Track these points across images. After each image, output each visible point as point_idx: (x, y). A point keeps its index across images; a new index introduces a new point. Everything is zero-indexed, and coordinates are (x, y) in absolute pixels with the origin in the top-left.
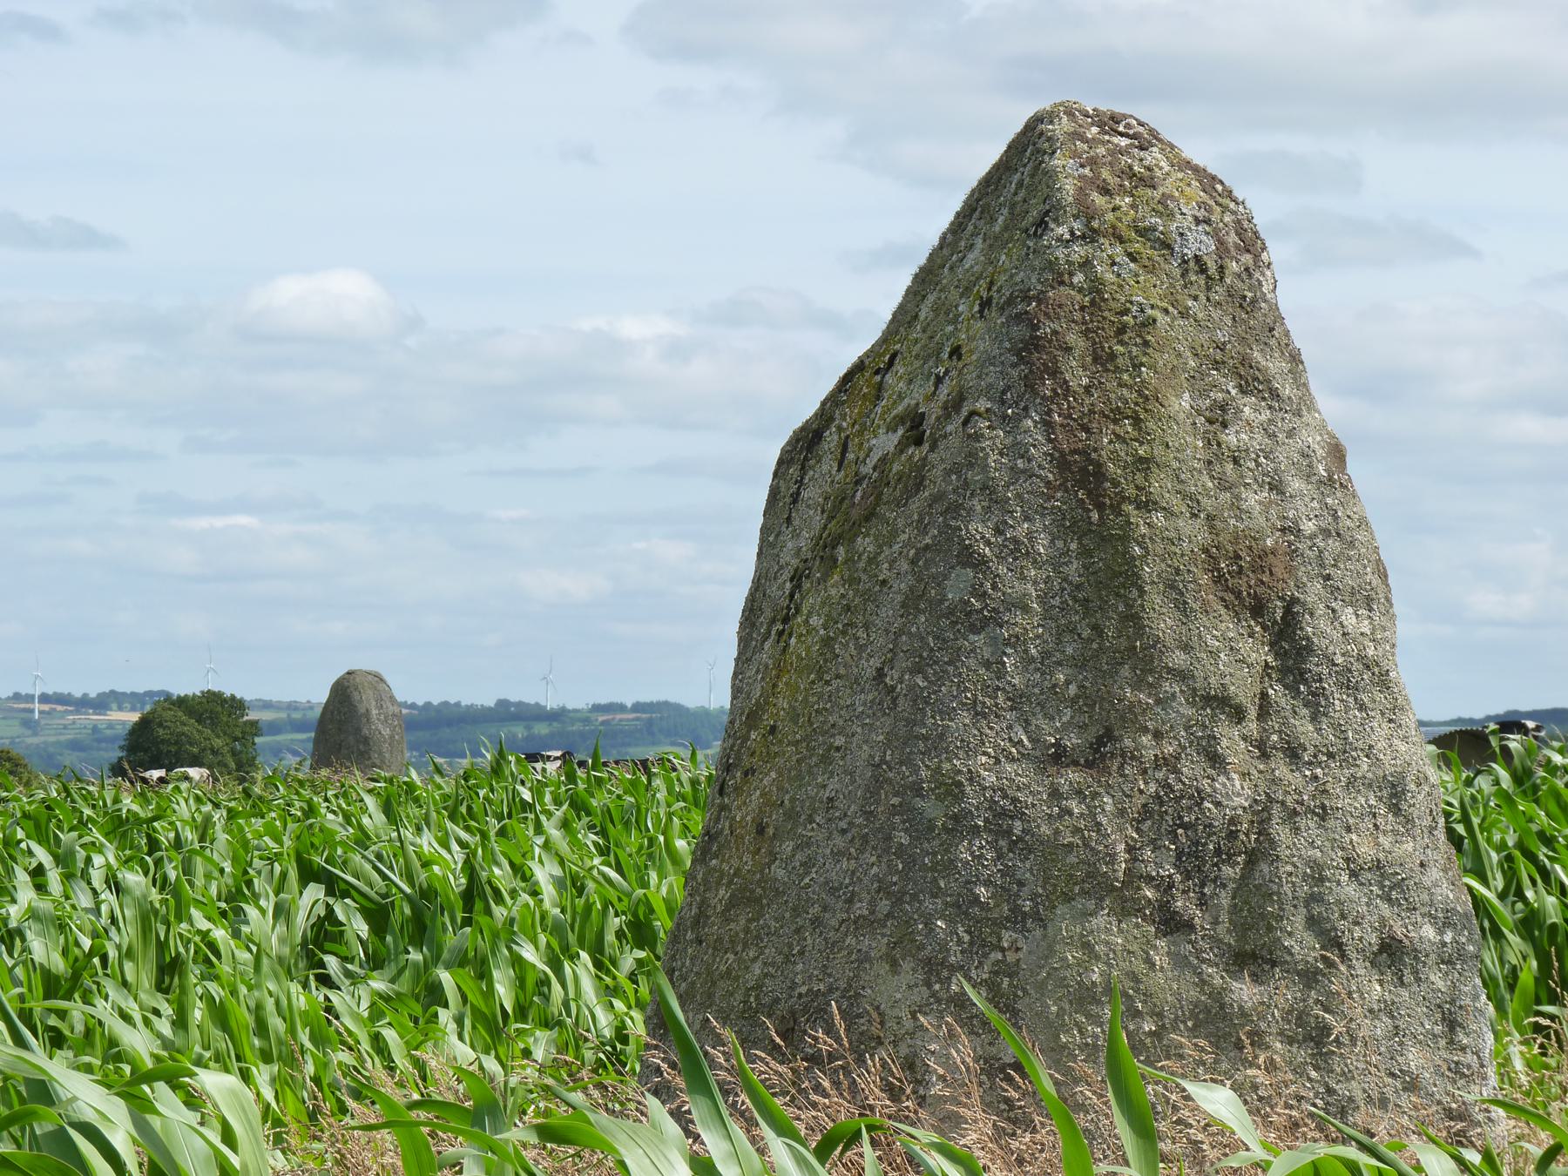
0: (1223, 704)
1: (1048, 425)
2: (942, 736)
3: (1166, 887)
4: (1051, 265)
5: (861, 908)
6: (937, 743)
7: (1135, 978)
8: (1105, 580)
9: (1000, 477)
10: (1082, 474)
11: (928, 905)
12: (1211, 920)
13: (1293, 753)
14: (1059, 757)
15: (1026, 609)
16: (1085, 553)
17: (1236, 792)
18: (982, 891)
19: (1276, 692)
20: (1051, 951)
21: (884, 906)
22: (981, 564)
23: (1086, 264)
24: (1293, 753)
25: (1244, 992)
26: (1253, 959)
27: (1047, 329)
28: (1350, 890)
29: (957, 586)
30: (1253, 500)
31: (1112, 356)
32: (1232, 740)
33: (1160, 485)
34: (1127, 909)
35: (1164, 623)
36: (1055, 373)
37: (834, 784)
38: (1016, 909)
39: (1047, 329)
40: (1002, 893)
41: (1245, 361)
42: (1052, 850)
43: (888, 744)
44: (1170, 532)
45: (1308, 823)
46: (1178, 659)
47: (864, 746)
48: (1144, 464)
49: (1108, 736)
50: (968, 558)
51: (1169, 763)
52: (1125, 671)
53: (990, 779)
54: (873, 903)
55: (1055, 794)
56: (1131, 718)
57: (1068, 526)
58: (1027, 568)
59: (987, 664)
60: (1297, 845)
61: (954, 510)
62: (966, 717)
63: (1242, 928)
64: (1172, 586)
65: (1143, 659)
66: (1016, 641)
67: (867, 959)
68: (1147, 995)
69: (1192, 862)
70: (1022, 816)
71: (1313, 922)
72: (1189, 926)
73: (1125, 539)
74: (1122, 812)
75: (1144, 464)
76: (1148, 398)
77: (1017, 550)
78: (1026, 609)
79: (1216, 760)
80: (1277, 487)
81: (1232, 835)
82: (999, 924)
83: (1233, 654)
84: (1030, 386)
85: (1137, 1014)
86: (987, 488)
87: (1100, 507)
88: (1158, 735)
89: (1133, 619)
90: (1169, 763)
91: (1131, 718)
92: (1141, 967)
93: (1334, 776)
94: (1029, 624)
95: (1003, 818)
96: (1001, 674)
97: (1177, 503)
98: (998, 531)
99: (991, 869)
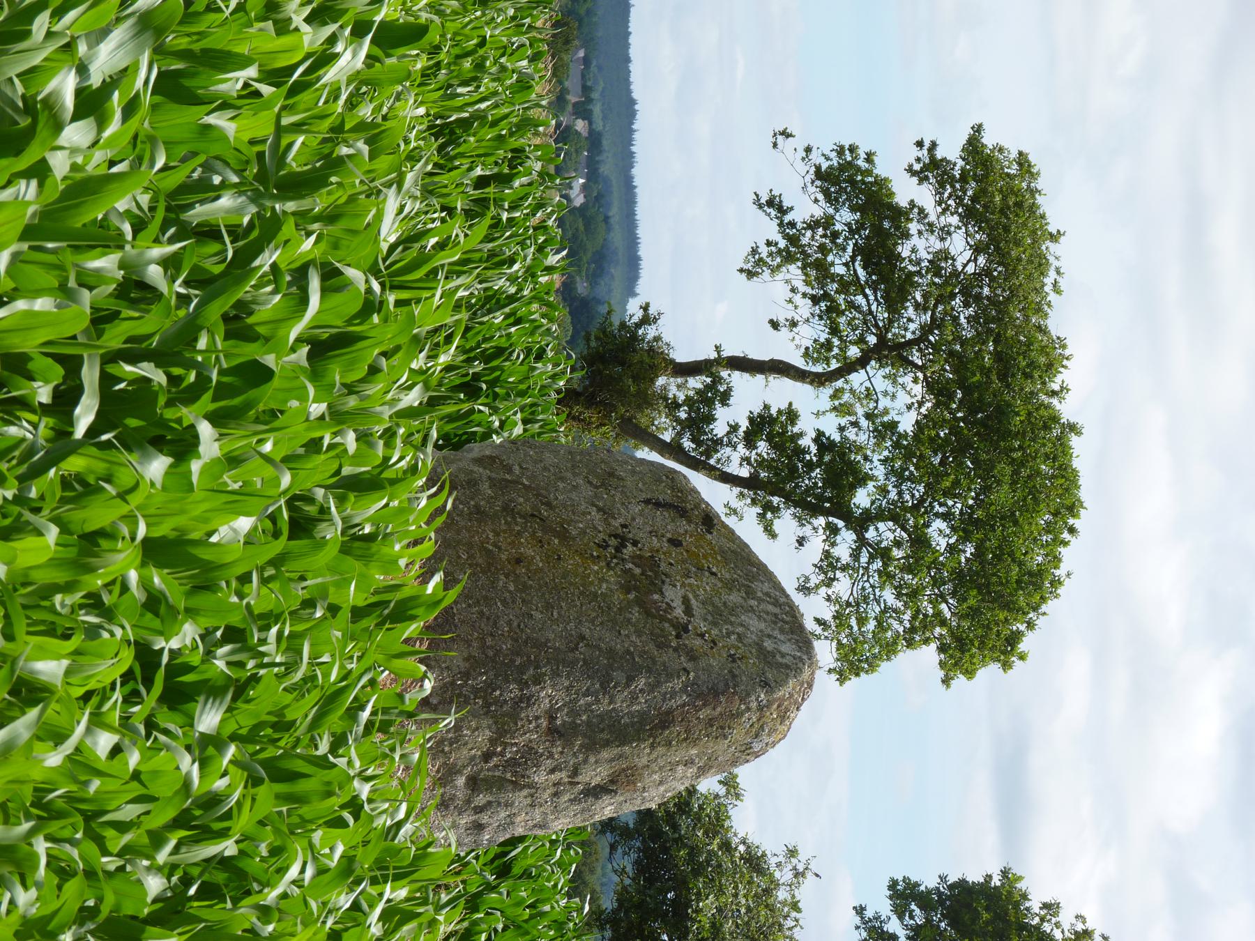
0: (575, 772)
1: (683, 705)
2: (558, 675)
3: (502, 754)
4: (748, 695)
5: (489, 641)
6: (556, 674)
7: (466, 744)
8: (620, 732)
9: (663, 689)
10: (665, 721)
11: (491, 673)
12: (487, 770)
13: (556, 794)
14: (552, 718)
15: (610, 703)
16: (633, 724)
17: (540, 777)
18: (498, 693)
19: (581, 787)
20: (474, 717)
21: (491, 653)
22: (628, 685)
23: (748, 709)
24: (556, 794)
25: (461, 781)
26: (474, 783)
27: (722, 699)
28: (503, 815)
29: (619, 676)
30: (656, 777)
31: (712, 726)
32: (563, 775)
33: (661, 750)
34: (493, 741)
35: (605, 754)
36: (704, 705)
37: (538, 615)
38: (491, 704)
39: (722, 699)
40: (496, 701)
41: (711, 767)
42: (514, 717)
43: (556, 649)
44: (641, 754)
45: (529, 801)
46: (592, 759)
47: (554, 635)
48: (669, 744)
49: (561, 735)
50: (630, 679)
51: (551, 756)
52: (587, 741)
53: (543, 694)
54: (491, 647)
55: (537, 718)
56: (568, 743)
57: (643, 716)
58: (625, 702)
59: (588, 690)
60: (520, 798)
61: (649, 671)
62: (567, 683)
63: (485, 780)
64: (621, 756)
65: (592, 746)
66: (598, 701)
67: (469, 646)
68: (459, 749)
69: (512, 763)
70: (528, 706)
71: (489, 803)
72: (486, 762)
73: (639, 740)
74: (530, 741)
75: (669, 744)
76: (695, 742)
77: (634, 698)
78: (610, 703)
79: (552, 771)
80: (661, 783)
81: (523, 776)
82: (484, 698)
83: (595, 774)
84: (698, 697)
85: (451, 745)
86: (658, 684)
87: (651, 729)
88: (562, 753)
89: (607, 744)
90: (551, 756)
91: (568, 743)
92: (469, 746)
93: (548, 808)
94: (604, 706)
95: (528, 700)
96: (585, 695)
97: (654, 756)
98: (641, 690)
99: (508, 696)
